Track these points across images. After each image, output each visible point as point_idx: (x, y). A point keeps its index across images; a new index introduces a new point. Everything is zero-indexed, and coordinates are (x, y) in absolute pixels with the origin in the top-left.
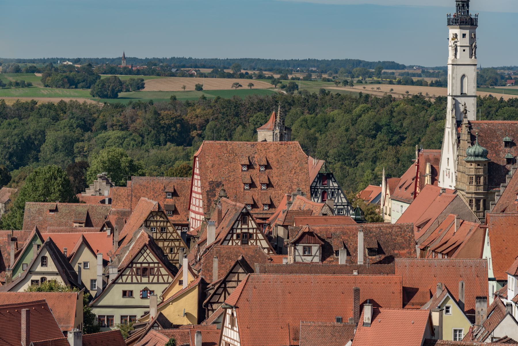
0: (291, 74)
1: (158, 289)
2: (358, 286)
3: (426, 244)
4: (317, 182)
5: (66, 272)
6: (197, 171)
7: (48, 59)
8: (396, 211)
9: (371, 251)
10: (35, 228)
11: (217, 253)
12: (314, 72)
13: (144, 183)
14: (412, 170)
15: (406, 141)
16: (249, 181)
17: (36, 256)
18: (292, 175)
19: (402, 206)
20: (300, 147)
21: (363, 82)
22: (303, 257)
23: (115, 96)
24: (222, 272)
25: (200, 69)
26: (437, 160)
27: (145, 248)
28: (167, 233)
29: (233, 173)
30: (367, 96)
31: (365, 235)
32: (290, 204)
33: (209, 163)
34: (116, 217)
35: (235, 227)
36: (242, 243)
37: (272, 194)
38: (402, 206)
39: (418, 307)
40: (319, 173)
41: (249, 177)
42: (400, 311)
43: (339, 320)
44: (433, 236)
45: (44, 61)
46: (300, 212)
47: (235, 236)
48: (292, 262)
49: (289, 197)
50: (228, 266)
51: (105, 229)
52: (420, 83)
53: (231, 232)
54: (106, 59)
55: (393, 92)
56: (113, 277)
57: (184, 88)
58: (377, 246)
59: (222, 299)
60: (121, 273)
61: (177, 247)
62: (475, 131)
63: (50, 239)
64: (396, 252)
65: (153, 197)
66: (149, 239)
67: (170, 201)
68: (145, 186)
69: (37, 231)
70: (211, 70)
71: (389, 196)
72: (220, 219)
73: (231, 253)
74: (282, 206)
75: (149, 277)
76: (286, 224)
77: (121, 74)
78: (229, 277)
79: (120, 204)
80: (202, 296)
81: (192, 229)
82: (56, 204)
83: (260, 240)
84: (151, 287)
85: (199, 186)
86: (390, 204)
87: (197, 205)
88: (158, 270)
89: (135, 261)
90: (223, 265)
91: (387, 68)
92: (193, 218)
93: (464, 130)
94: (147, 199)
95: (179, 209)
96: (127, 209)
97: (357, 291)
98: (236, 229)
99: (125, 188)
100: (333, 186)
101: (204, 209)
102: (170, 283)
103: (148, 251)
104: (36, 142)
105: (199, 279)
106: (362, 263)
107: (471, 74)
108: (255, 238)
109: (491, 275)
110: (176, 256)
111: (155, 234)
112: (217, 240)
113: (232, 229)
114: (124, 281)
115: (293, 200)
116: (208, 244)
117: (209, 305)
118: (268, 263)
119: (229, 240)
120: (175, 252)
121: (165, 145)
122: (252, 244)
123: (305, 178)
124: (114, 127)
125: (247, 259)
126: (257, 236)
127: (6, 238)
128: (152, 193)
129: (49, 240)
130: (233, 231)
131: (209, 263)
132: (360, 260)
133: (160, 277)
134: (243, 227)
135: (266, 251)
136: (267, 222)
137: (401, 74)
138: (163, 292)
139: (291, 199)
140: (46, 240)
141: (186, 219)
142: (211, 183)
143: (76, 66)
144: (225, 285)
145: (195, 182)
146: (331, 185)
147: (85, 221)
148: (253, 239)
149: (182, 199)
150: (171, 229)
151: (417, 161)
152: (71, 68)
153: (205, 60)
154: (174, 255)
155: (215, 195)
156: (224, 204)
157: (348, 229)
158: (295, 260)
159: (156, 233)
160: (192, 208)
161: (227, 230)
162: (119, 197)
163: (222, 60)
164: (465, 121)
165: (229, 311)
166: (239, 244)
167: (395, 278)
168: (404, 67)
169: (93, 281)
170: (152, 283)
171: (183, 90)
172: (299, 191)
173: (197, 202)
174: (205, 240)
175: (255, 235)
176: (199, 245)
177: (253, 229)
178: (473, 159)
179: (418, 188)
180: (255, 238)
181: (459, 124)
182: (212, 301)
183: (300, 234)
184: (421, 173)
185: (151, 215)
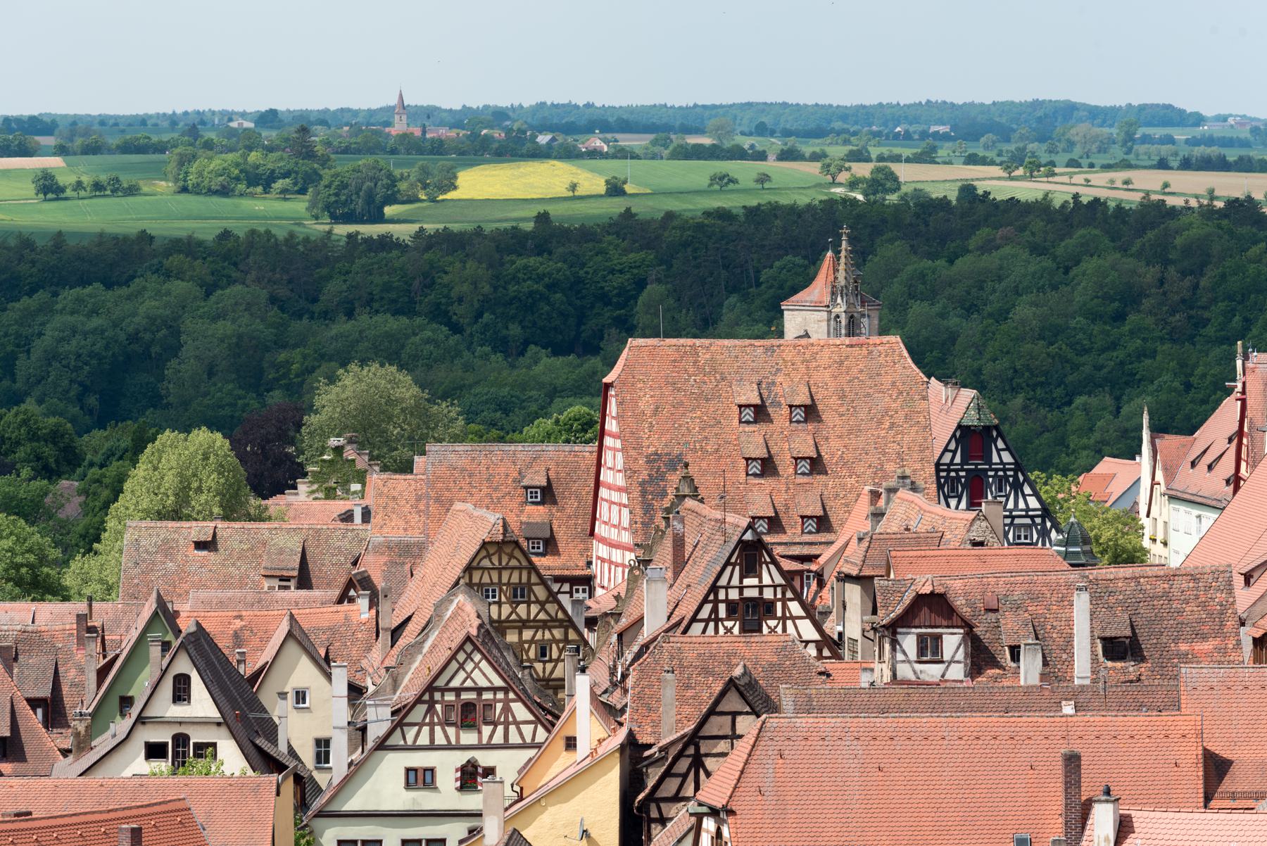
0: (879, 144)
1: (507, 764)
2: (1077, 747)
4: (954, 452)
5: (243, 718)
6: (611, 425)
7: (186, 113)
8: (1182, 531)
9: (1117, 648)
10: (154, 595)
11: (672, 658)
12: (945, 137)
13: (463, 462)
14: (1225, 417)
15: (1210, 330)
16: (762, 453)
17: (158, 674)
18: (883, 433)
19: (1199, 517)
20: (905, 354)
21: (1085, 162)
22: (918, 667)
23: (379, 218)
24: (687, 710)
25: (618, 136)
27: (469, 647)
28: (529, 603)
29: (716, 430)
30: (1096, 201)
31: (1096, 600)
32: (878, 515)
33: (646, 404)
34: (384, 559)
35: (723, 581)
36: (743, 630)
37: (826, 486)
38: (1199, 517)
39: (1250, 803)
40: (959, 426)
41: (762, 441)
42: (1197, 816)
45: (173, 120)
46: (910, 538)
47: (722, 612)
48: (887, 677)
49: (875, 495)
50: (705, 695)
51: (352, 593)
52: (1245, 165)
53: (711, 597)
54: (349, 110)
55: (1167, 190)
56: (375, 732)
57: (573, 187)
58: (1128, 633)
59: (689, 790)
60: (400, 717)
61: (557, 642)
63: (198, 624)
64: (1184, 647)
65: (487, 501)
66: (477, 622)
67: (538, 514)
68: (463, 470)
69: (161, 602)
70: (652, 136)
71: (1163, 488)
72: (679, 563)
73: (712, 656)
74: (853, 523)
75: (480, 732)
76: (867, 572)
77: (394, 151)
78: (706, 726)
79: (396, 521)
80: (631, 783)
81: (599, 592)
82: (212, 524)
83: (793, 618)
84: (485, 759)
85: (620, 466)
86: (1165, 510)
87: (616, 522)
88: (507, 709)
89: (441, 683)
90: (690, 693)
91: (1149, 124)
92: (603, 560)
94: (469, 506)
95: (561, 535)
96: (414, 536)
97: (1072, 762)
98: (727, 588)
99: (409, 477)
100: (1001, 462)
101: (635, 533)
102: (539, 746)
103: (477, 657)
104: (155, 349)
105: (622, 734)
106: (1087, 682)
108: (779, 614)
110: (555, 667)
111: (494, 609)
112: (673, 621)
113: (714, 588)
114: (410, 742)
115: (887, 503)
116: (647, 633)
117: (653, 807)
118: (820, 684)
119: (707, 621)
120: (555, 656)
121: (522, 353)
122: (772, 630)
123: (920, 440)
124: (376, 305)
125: (758, 674)
126: (784, 607)
127: (71, 624)
128: (485, 490)
129: (193, 629)
130: (716, 595)
131: (651, 686)
133: (512, 728)
134: (747, 582)
135: (812, 651)
136: (814, 567)
138: (519, 772)
139: (882, 503)
140: (186, 625)
141: (582, 563)
142: (653, 459)
143: (264, 133)
144: (697, 748)
145: (608, 457)
146: (995, 459)
147: (295, 573)
148: (775, 617)
149: (571, 505)
150: (540, 592)
151: (1240, 385)
152: (249, 141)
153: (630, 110)
154: (549, 666)
155: (664, 494)
156: (689, 518)
157: (1047, 584)
158: (894, 675)
159: (499, 604)
160: (600, 529)
162: (391, 504)
163: (680, 108)
165: (709, 824)
166: (736, 630)
167: (1181, 723)
168: (1198, 119)
169: (323, 748)
170: (490, 747)
171: (571, 194)
172: (904, 477)
173: (616, 517)
174: (639, 622)
175: (779, 605)
176: (620, 636)
177: (775, 587)
179: (1243, 465)
180: (779, 614)
182: (660, 794)
183: (908, 598)
184: (1251, 422)
185: (483, 553)
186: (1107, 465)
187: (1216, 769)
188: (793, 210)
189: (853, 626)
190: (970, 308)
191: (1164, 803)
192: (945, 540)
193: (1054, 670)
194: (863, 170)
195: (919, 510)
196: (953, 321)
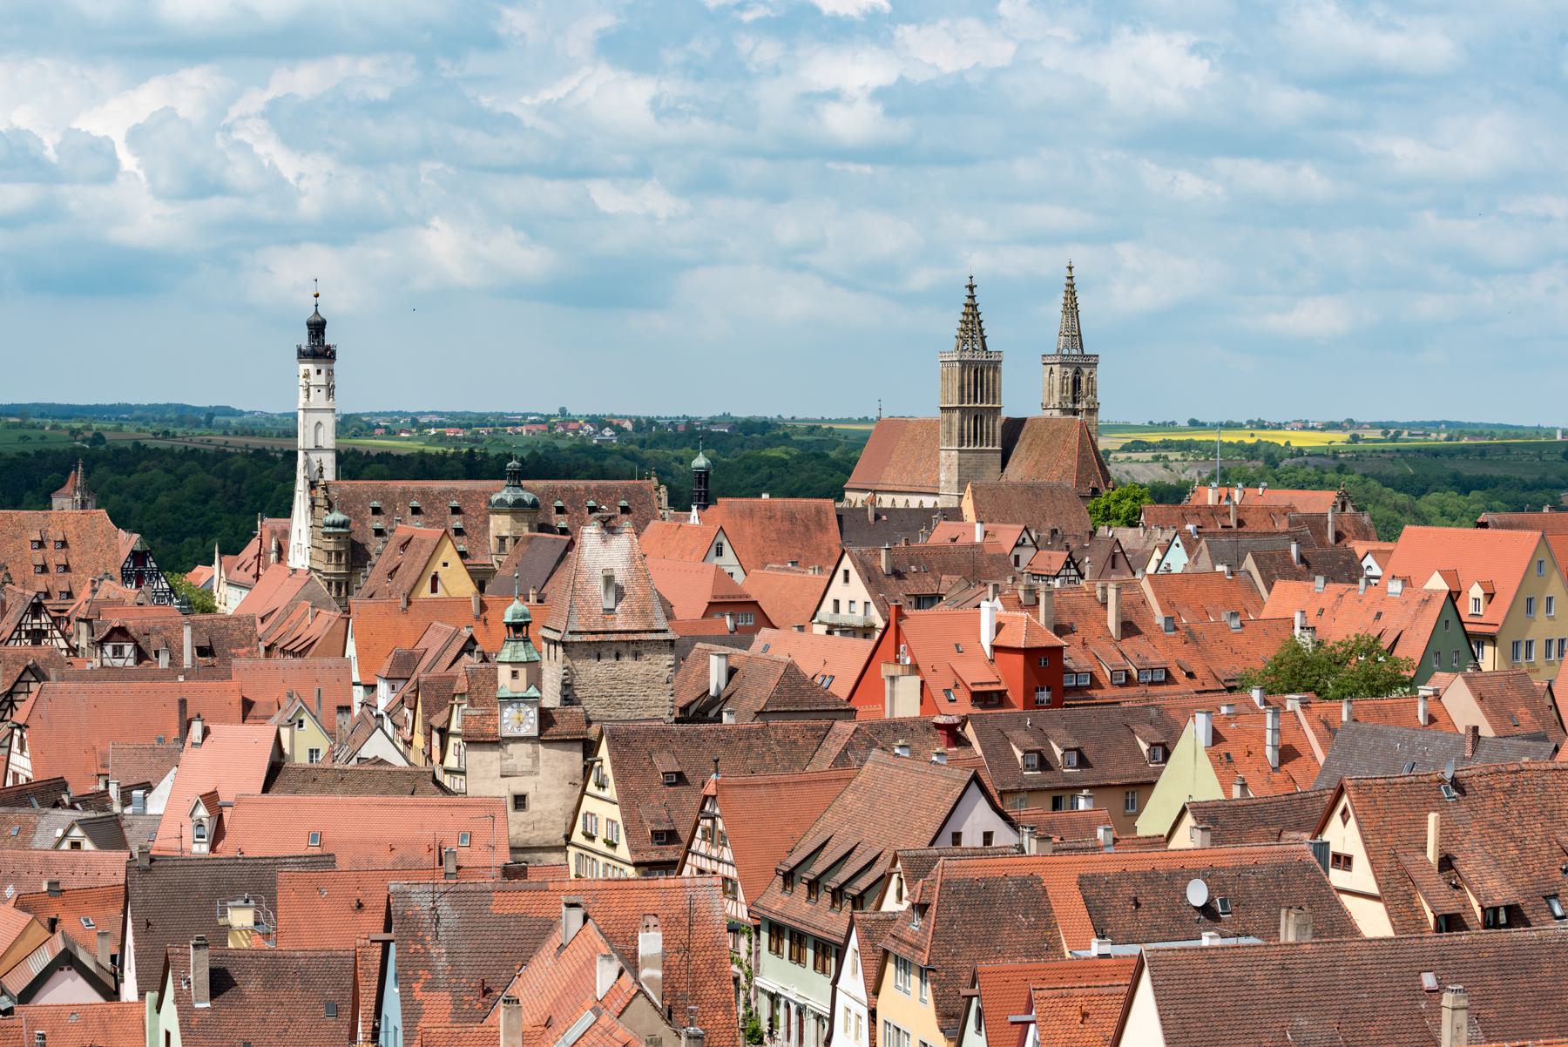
3: (272, 640)
9: (202, 651)
14: (253, 547)
15: (246, 508)
16: (41, 562)
26: (286, 534)
31: (194, 629)
32: (94, 591)
43: (160, 740)
44: (281, 630)
46: (109, 602)
49: (93, 582)
59: (8, 716)
62: (334, 493)
74: (83, 595)
93: (320, 493)
97: (183, 703)
107: (329, 421)
109: (356, 678)
113: (20, 624)
118: (68, 669)
132: (187, 660)
137: (242, 425)
161: (13, 626)
164: (322, 482)
165: (17, 732)
167: (232, 685)
168: (241, 413)
178: (331, 530)
181: (313, 485)
186: (199, 569)
187: (247, 705)
188: (58, 454)
189: (83, 641)
190: (137, 497)
191: (224, 720)
192: (127, 603)
193: (175, 661)
194: (89, 434)
195: (113, 589)
196: (130, 503)
